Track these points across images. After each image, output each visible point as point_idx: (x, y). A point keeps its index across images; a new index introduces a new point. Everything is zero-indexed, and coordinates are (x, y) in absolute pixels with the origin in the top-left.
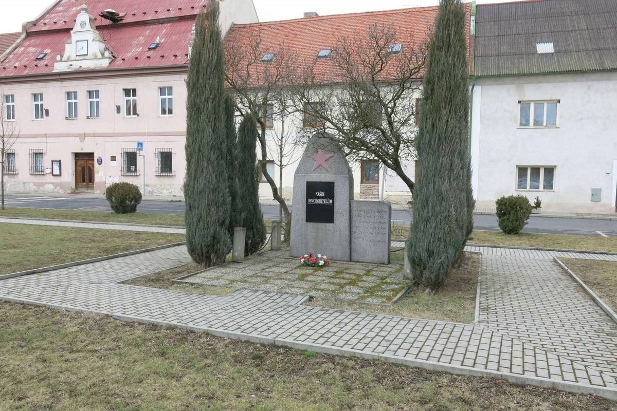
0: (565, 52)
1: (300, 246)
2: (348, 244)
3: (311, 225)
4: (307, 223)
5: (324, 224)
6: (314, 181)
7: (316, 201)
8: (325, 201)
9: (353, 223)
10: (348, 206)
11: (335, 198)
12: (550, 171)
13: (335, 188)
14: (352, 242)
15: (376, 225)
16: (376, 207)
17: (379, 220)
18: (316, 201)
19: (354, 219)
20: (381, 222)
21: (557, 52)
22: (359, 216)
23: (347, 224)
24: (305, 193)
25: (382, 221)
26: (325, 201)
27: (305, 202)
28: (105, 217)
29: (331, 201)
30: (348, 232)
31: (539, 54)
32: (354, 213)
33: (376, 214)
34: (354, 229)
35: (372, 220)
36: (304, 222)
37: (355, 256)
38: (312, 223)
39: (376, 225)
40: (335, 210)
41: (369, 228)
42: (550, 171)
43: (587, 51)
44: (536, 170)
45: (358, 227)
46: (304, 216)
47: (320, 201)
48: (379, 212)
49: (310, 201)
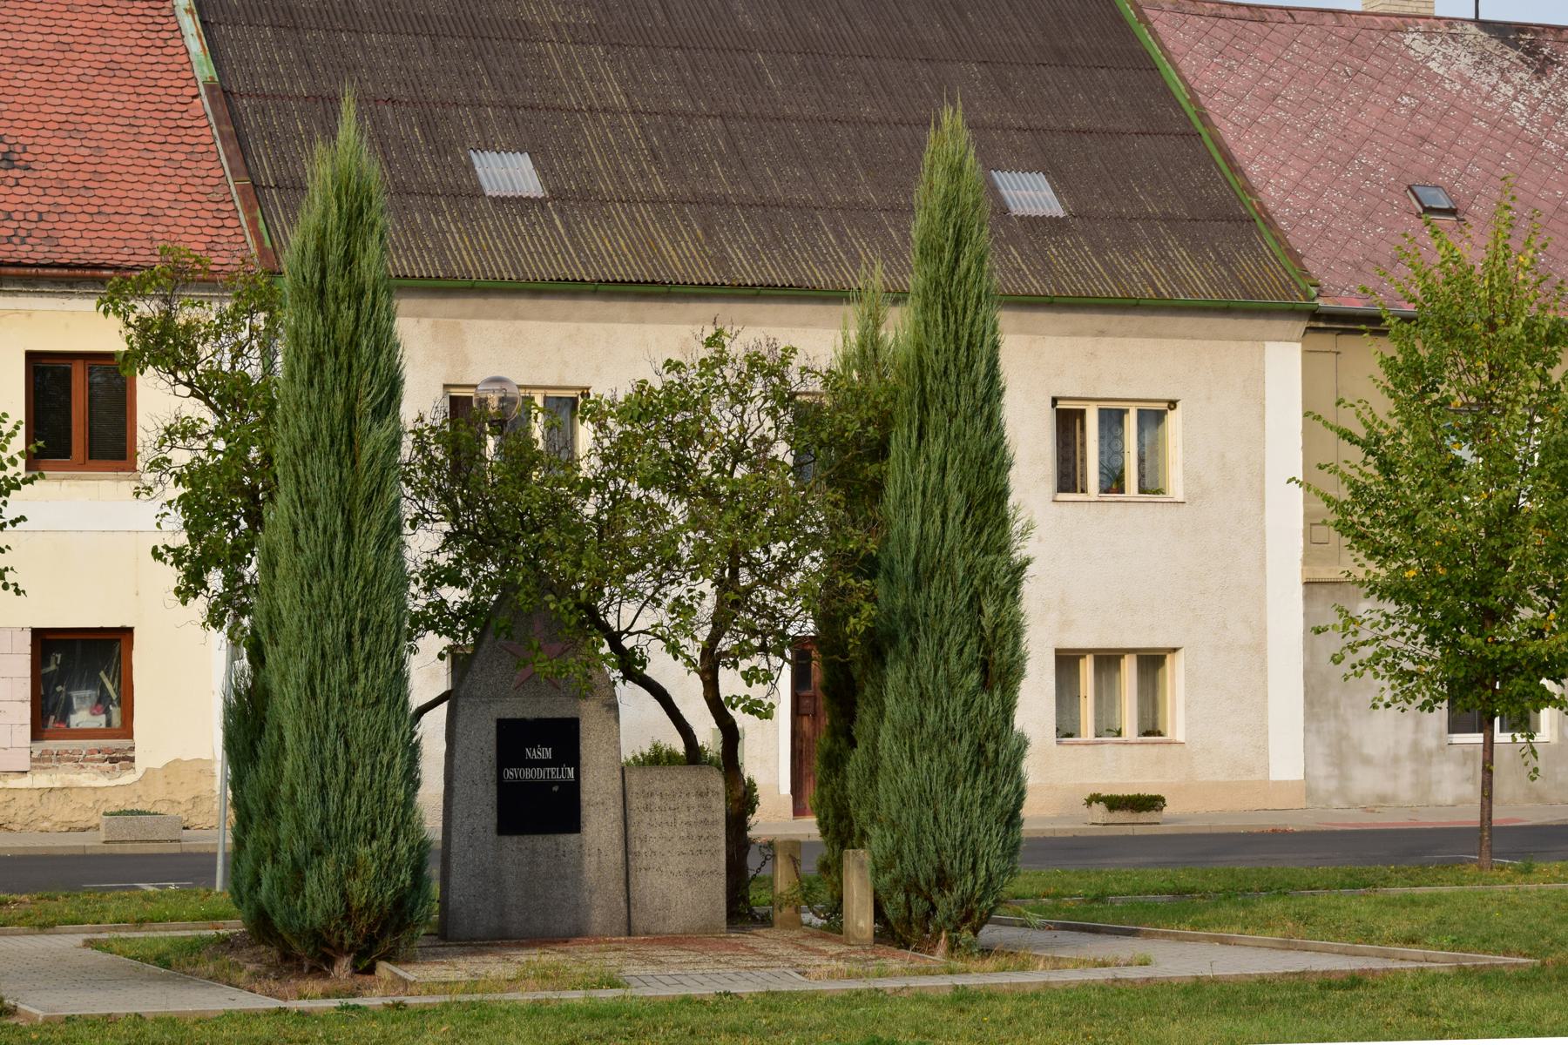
0: (585, 197)
1: (479, 906)
2: (622, 885)
3: (511, 842)
4: (502, 837)
5: (551, 836)
6: (29, 650)
7: (528, 774)
8: (553, 773)
9: (632, 829)
10: (619, 782)
11: (583, 760)
12: (1152, 662)
13: (582, 735)
14: (632, 879)
15: (694, 831)
16: (693, 780)
17: (701, 816)
18: (528, 774)
19: (634, 818)
20: (705, 822)
21: (557, 195)
22: (647, 808)
23: (617, 834)
24: (492, 752)
25: (710, 819)
26: (553, 773)
27: (491, 775)
28: (1360, 982)
29: (571, 772)
30: (620, 855)
31: (495, 200)
32: (636, 802)
33: (693, 800)
34: (636, 846)
35: (682, 816)
36: (492, 834)
37: (639, 922)
38: (515, 838)
39: (694, 831)
40: (584, 797)
41: (676, 839)
42: (1152, 662)
43: (656, 200)
44: (1107, 660)
45: (644, 840)
46: (491, 819)
47: (540, 774)
48: (700, 795)
49: (511, 773)
